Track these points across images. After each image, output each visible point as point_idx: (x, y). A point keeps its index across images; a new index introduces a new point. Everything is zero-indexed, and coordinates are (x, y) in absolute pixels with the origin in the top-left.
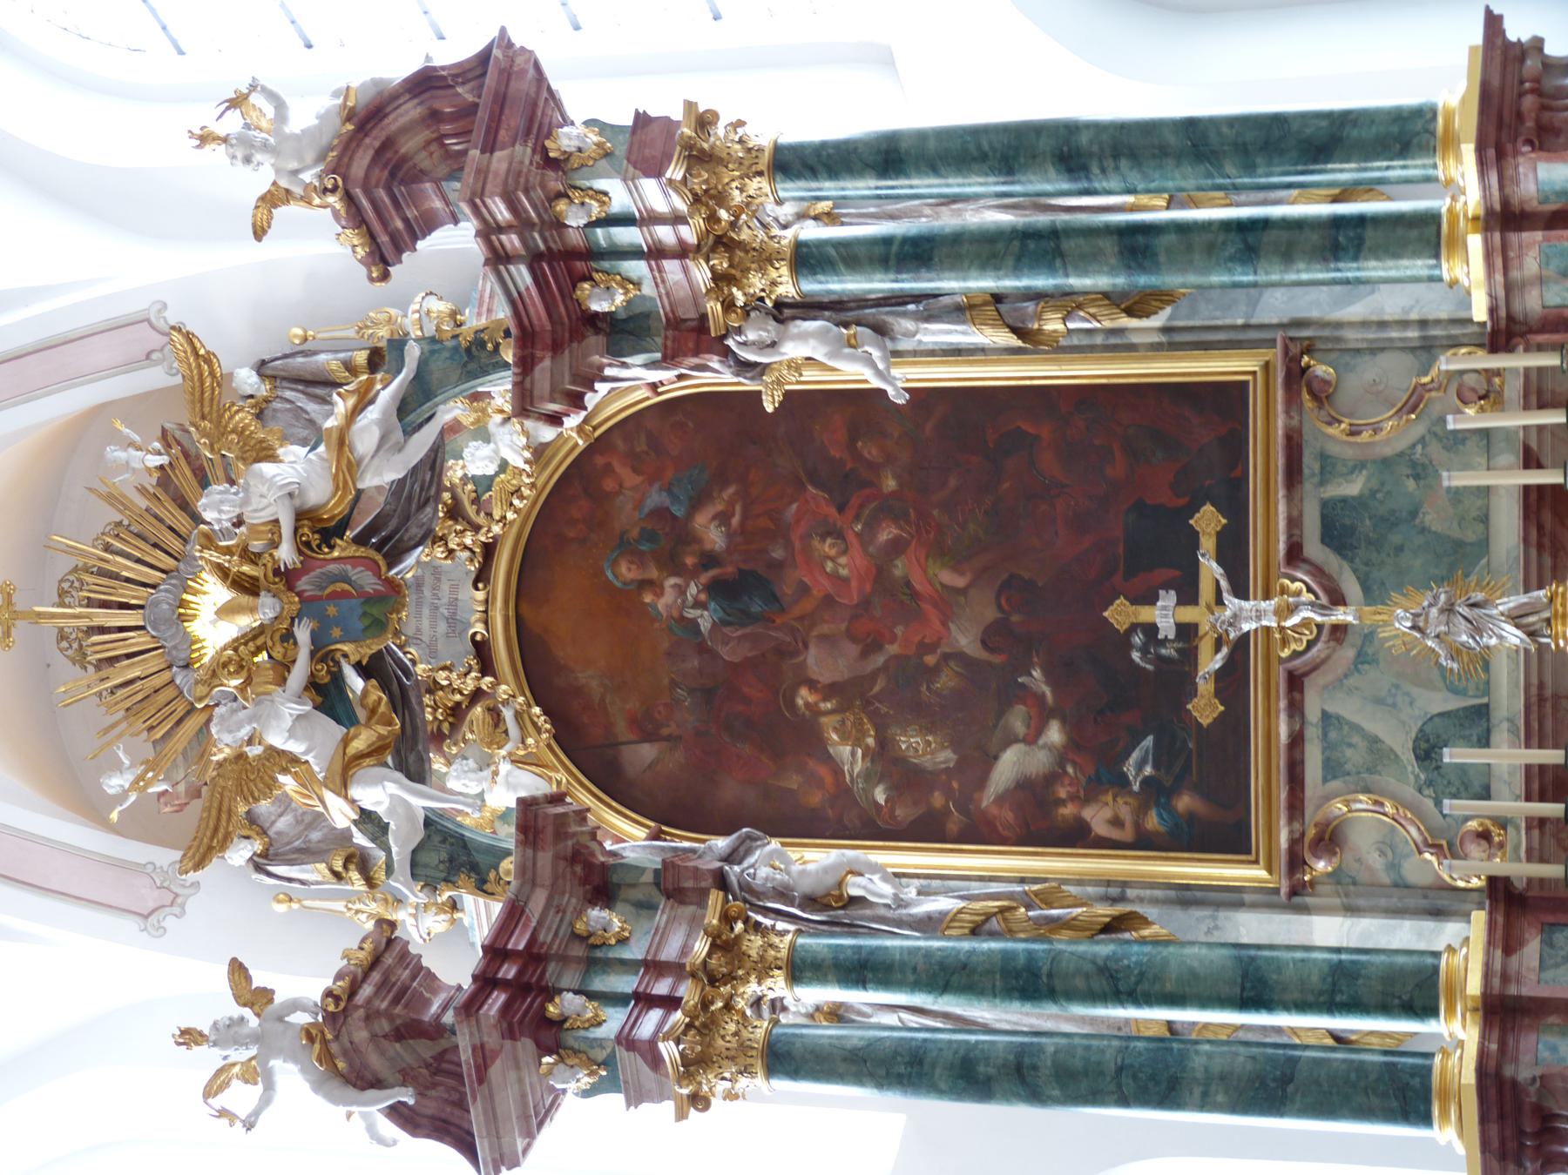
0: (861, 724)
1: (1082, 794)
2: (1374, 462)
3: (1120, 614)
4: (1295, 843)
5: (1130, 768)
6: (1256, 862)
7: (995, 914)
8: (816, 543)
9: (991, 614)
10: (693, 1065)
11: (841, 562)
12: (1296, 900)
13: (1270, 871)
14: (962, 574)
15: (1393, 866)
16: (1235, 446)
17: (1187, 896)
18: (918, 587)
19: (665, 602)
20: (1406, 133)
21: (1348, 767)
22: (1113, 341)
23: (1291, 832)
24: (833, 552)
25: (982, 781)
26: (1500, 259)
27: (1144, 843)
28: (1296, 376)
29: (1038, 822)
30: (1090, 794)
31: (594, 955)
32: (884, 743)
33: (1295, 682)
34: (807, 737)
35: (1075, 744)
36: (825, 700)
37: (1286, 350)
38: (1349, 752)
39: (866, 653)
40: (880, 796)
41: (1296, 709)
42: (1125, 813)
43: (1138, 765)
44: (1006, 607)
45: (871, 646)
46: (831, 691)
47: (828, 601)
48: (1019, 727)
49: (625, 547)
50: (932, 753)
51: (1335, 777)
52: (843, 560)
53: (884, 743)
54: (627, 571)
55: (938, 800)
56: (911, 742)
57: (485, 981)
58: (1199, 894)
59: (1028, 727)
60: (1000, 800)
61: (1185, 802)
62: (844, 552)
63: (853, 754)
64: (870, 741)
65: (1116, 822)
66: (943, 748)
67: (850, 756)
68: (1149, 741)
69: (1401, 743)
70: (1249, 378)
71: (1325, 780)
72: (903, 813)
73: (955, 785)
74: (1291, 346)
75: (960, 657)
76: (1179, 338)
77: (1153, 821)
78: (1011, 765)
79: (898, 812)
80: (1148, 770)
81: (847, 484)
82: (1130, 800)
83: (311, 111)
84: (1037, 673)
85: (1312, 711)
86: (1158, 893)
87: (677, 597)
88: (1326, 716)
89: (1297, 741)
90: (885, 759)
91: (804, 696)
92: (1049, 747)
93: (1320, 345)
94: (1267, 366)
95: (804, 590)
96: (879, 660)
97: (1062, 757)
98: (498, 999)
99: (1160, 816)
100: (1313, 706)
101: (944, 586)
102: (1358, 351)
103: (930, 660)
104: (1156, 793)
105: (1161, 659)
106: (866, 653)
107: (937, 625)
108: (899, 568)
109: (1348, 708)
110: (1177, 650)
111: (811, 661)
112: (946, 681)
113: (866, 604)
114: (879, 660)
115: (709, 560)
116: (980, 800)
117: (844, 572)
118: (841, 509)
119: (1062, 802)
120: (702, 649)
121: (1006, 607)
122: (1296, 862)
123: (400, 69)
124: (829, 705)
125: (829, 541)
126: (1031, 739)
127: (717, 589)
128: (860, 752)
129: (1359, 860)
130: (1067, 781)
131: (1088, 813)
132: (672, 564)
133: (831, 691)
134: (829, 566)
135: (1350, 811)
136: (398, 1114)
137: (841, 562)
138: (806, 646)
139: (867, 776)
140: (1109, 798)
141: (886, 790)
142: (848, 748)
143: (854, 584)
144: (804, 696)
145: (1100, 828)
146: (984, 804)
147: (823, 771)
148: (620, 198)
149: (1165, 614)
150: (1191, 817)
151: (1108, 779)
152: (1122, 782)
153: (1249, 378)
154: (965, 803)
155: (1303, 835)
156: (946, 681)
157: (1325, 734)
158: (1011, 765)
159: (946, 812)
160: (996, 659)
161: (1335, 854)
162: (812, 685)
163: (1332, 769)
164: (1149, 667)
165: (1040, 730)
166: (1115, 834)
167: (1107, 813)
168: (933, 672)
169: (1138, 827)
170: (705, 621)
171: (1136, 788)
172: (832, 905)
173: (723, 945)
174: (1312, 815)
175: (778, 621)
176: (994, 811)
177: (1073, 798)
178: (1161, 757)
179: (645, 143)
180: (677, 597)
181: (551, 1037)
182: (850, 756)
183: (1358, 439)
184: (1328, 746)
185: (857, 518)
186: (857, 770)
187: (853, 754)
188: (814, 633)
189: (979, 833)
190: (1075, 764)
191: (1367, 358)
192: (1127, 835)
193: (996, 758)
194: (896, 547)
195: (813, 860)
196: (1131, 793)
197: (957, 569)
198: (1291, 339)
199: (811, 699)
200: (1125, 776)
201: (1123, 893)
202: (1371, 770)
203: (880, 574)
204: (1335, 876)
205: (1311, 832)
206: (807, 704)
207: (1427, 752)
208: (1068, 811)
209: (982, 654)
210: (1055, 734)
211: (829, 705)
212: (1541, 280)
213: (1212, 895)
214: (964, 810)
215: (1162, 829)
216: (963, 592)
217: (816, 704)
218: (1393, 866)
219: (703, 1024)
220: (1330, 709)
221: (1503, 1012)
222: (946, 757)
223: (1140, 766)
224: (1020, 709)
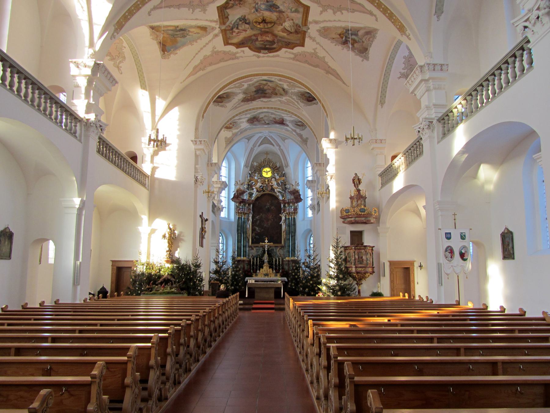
3: (266, 238)
10: (238, 213)
11: (270, 217)
16: (278, 243)
17: (249, 240)
19: (268, 204)
20: (294, 255)
26: (287, 261)
29: (253, 230)
31: (245, 205)
34: (259, 215)
43: (257, 237)
57: (243, 199)
78: (257, 228)
87: (268, 205)
90: (257, 220)
104: (255, 238)
122: (251, 247)
136: (235, 194)
137: (270, 217)
149: (266, 241)
151: (256, 235)
158: (257, 228)
172: (248, 219)
173: (246, 213)
179: (296, 209)
180: (268, 205)
181: (240, 203)
182: (257, 217)
189: (253, 226)
195: (251, 218)
219: (241, 213)
221: (244, 261)
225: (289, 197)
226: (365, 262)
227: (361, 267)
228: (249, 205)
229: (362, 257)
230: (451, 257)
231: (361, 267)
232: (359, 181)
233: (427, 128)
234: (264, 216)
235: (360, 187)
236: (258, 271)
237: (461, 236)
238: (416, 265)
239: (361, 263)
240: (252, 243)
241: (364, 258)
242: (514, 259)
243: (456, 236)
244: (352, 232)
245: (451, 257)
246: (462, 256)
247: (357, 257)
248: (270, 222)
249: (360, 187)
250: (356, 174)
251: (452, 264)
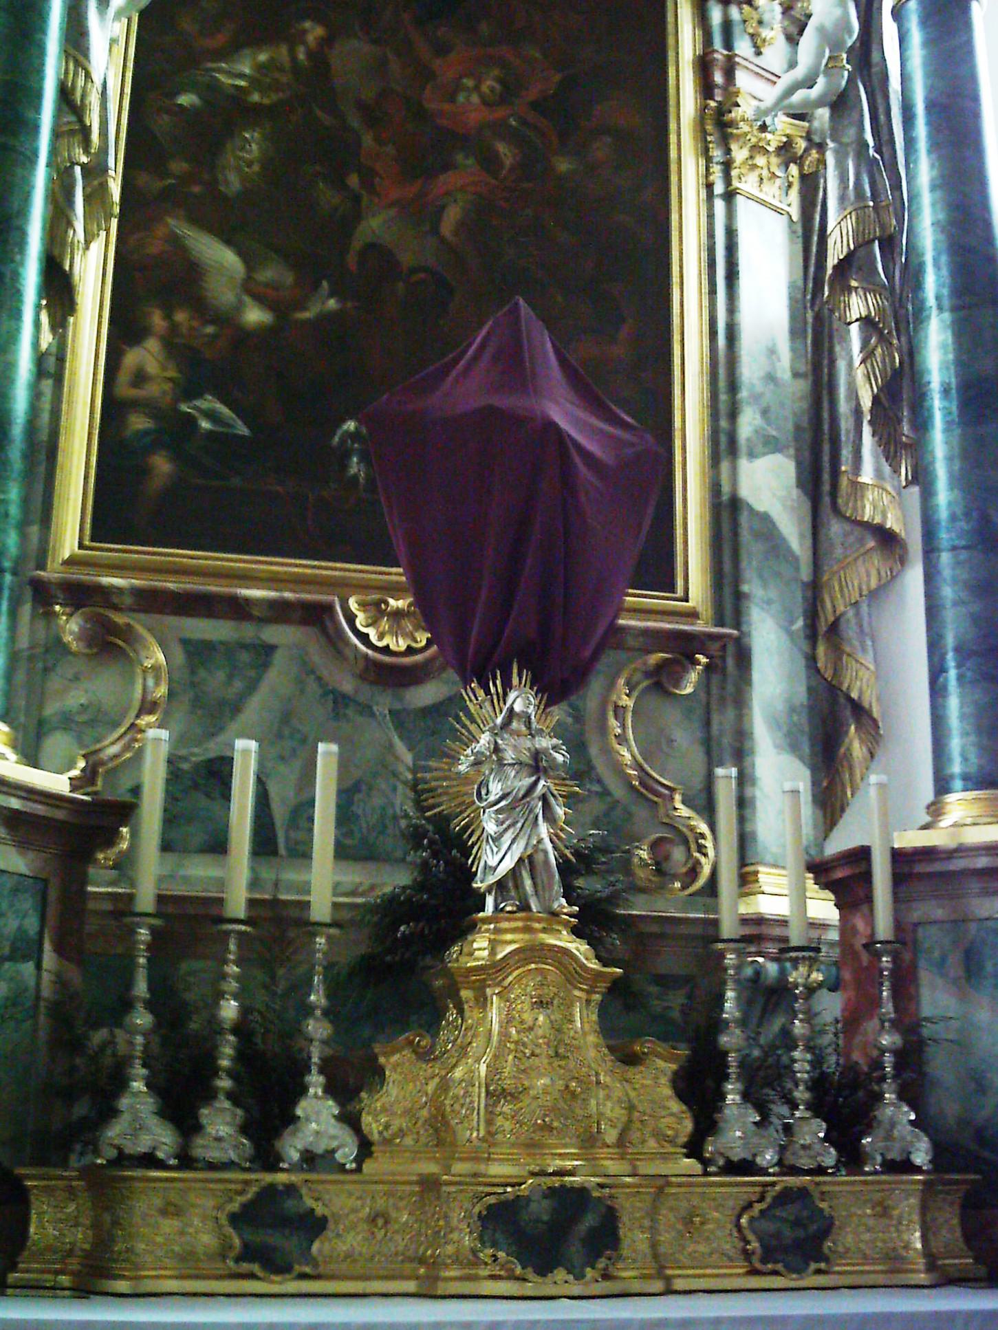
0: (278, 90)
1: (177, 340)
2: (582, 735)
4: (105, 595)
5: (209, 402)
6: (81, 546)
7: (81, 120)
8: (496, 72)
9: (407, 259)
11: (472, 100)
12: (28, 593)
13: (71, 562)
14: (456, 233)
15: (67, 722)
18: (442, 178)
21: (202, 673)
22: (723, 439)
23: (120, 590)
24: (485, 88)
25: (199, 221)
27: (113, 408)
32: (253, 115)
35: (242, 338)
36: (310, 54)
37: (712, 637)
38: (221, 675)
39: (361, 106)
40: (185, 99)
41: (279, 612)
42: (153, 390)
43: (210, 412)
44: (415, 278)
45: (371, 115)
47: (425, 74)
48: (267, 274)
50: (239, 170)
51: (189, 654)
52: (475, 99)
53: (253, 115)
55: (178, 166)
56: (252, 145)
58: (42, 469)
59: (267, 285)
60: (175, 241)
61: (162, 465)
62: (485, 103)
63: (241, 76)
64: (256, 97)
65: (140, 378)
66: (244, 179)
67: (239, 71)
68: (242, 430)
70: (680, 592)
71: (185, 642)
72: (163, 123)
73: (196, 189)
74: (717, 645)
75: (356, 216)
76: (725, 515)
77: (139, 422)
78: (221, 259)
79: (165, 117)
80: (205, 425)
81: (563, 114)
82: (169, 398)
84: (332, 303)
85: (274, 634)
86: (45, 417)
88: (270, 649)
89: (238, 609)
90: (230, 112)
91: (314, 32)
92: (239, 307)
93: (716, 679)
94: (693, 615)
95: (442, 49)
96: (354, 122)
97: (227, 321)
99: (146, 433)
100: (280, 634)
101: (442, 209)
102: (707, 724)
103: (353, 180)
104: (175, 431)
105: (347, 455)
106: (361, 106)
107: (395, 194)
108: (466, 161)
110: (356, 476)
111: (355, 43)
112: (327, 197)
113: (421, 115)
114: (354, 122)
116: (175, 217)
117: (461, 98)
118: (534, 105)
119: (168, 316)
121: (415, 278)
122: (80, 595)
124: (301, 56)
125: (498, 87)
126: (250, 288)
128: (243, 83)
129: (77, 678)
130: (195, 323)
131: (152, 344)
134: (468, 82)
135: (145, 670)
138: (374, 42)
139: (211, 90)
140: (172, 373)
141: (193, 106)
142: (247, 71)
143: (446, 107)
144: (314, 32)
145: (132, 358)
146: (170, 221)
147: (219, 41)
150: (144, 471)
151: (196, 371)
152: (190, 393)
153: (680, 592)
154: (172, 199)
155: (116, 608)
156: (327, 197)
157: (244, 646)
159: (163, 173)
160: (352, 260)
161: (89, 646)
162: (327, 42)
163: (199, 653)
164: (336, 439)
165: (261, 299)
166: (123, 377)
167: (152, 368)
168: (339, 183)
169: (134, 405)
171: (184, 408)
174: (139, 624)
175: (406, 17)
176: (161, 231)
177: (174, 329)
178: (221, 441)
182: (239, 71)
183: (611, 714)
184: (230, 650)
185: (524, 122)
186: (221, 77)
187: (241, 76)
188: (390, 55)
190: (215, 337)
191: (699, 734)
192: (124, 390)
193: (229, 242)
194: (490, 162)
196: (177, 401)
197: (461, 225)
198: (724, 648)
199: (311, 38)
200: (199, 395)
201: (49, 376)
202: (196, 703)
204: (57, 646)
205: (120, 619)
206: (304, 32)
208: (157, 320)
209: (356, 245)
210: (255, 316)
211: (301, 56)
212: (959, 922)
213: (39, 488)
214: (165, 194)
215: (128, 433)
216: (435, 230)
217: (304, 43)
218: (67, 722)
220: (279, 658)
222: (233, 183)
223: (211, 415)
224: (289, 278)
234: (352, 58)
236: (317, 1119)
240: (111, 517)
248: (457, 192)
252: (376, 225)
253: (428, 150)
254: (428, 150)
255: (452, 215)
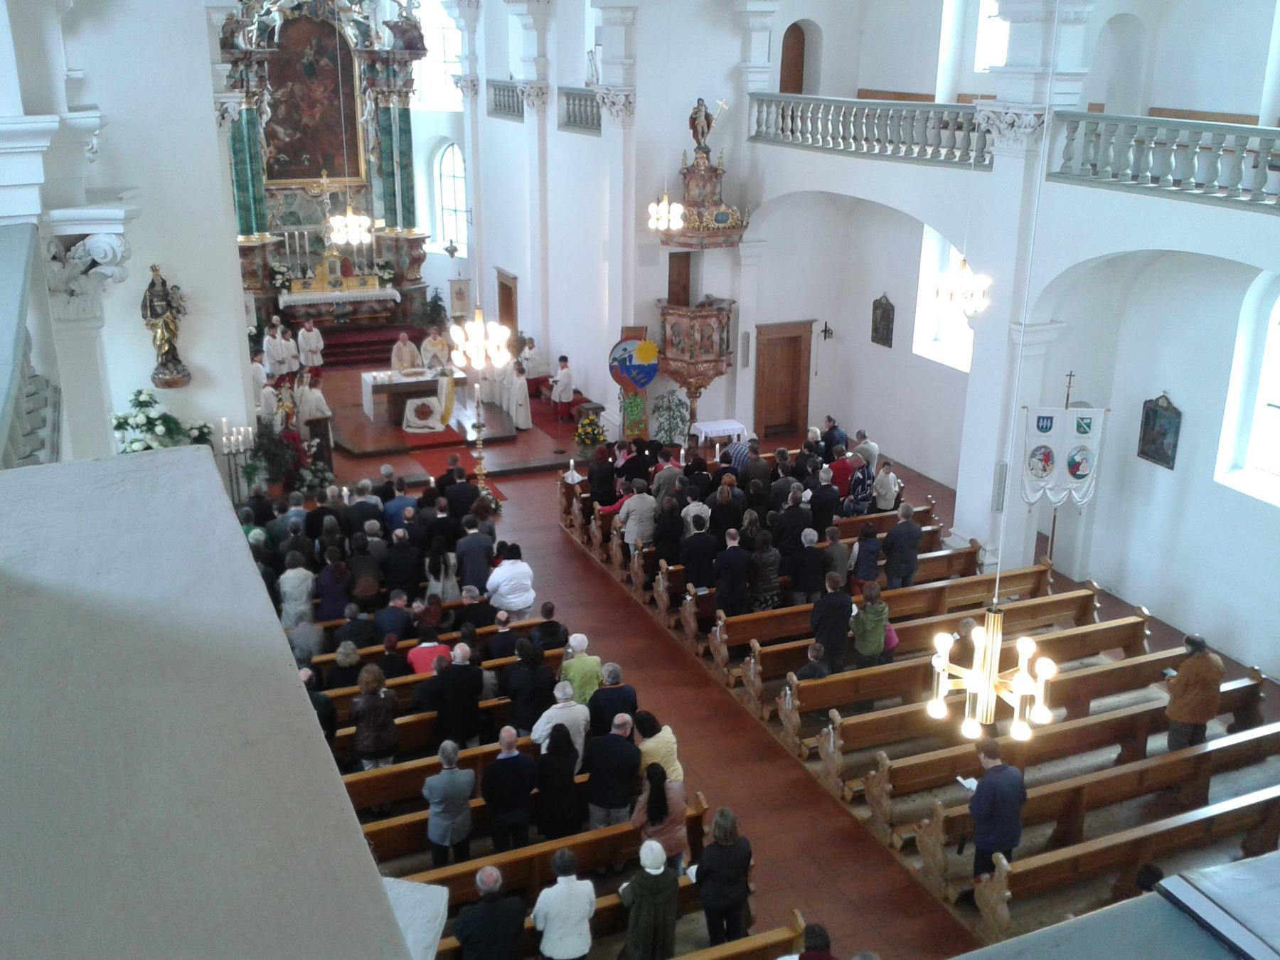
11: (319, 92)
20: (410, 221)
28: (362, 187)
30: (276, 147)
31: (249, 66)
33: (303, 189)
43: (283, 157)
46: (292, 90)
49: (319, 42)
54: (314, 42)
56: (282, 109)
61: (276, 167)
69: (293, 209)
78: (280, 130)
83: (416, 13)
91: (290, 84)
97: (283, 141)
98: (241, 56)
104: (277, 161)
109: (298, 200)
112: (296, 116)
115: (317, 61)
120: (299, 60)
123: (423, 32)
127: (311, 64)
132: (316, 53)
133: (292, 90)
137: (319, 92)
148: (401, 75)
151: (280, 150)
156: (296, 116)
158: (280, 130)
163: (286, 196)
170: (305, 60)
179: (409, 83)
203: (317, 101)
207: (292, 214)
210: (287, 139)
221: (263, 246)
225: (385, 41)
226: (716, 347)
227: (707, 362)
228: (260, 63)
229: (710, 337)
230: (1045, 470)
231: (707, 362)
232: (708, 118)
233: (1029, 135)
235: (708, 141)
237: (1079, 426)
238: (817, 329)
239: (707, 352)
241: (716, 337)
242: (1172, 468)
243: (1065, 421)
244: (672, 256)
245: (1045, 470)
246: (1074, 468)
247: (698, 336)
248: (318, 110)
249: (708, 141)
250: (700, 101)
251: (1043, 484)
252: (305, 120)
253: (313, 103)
254: (313, 103)
255: (318, 116)
